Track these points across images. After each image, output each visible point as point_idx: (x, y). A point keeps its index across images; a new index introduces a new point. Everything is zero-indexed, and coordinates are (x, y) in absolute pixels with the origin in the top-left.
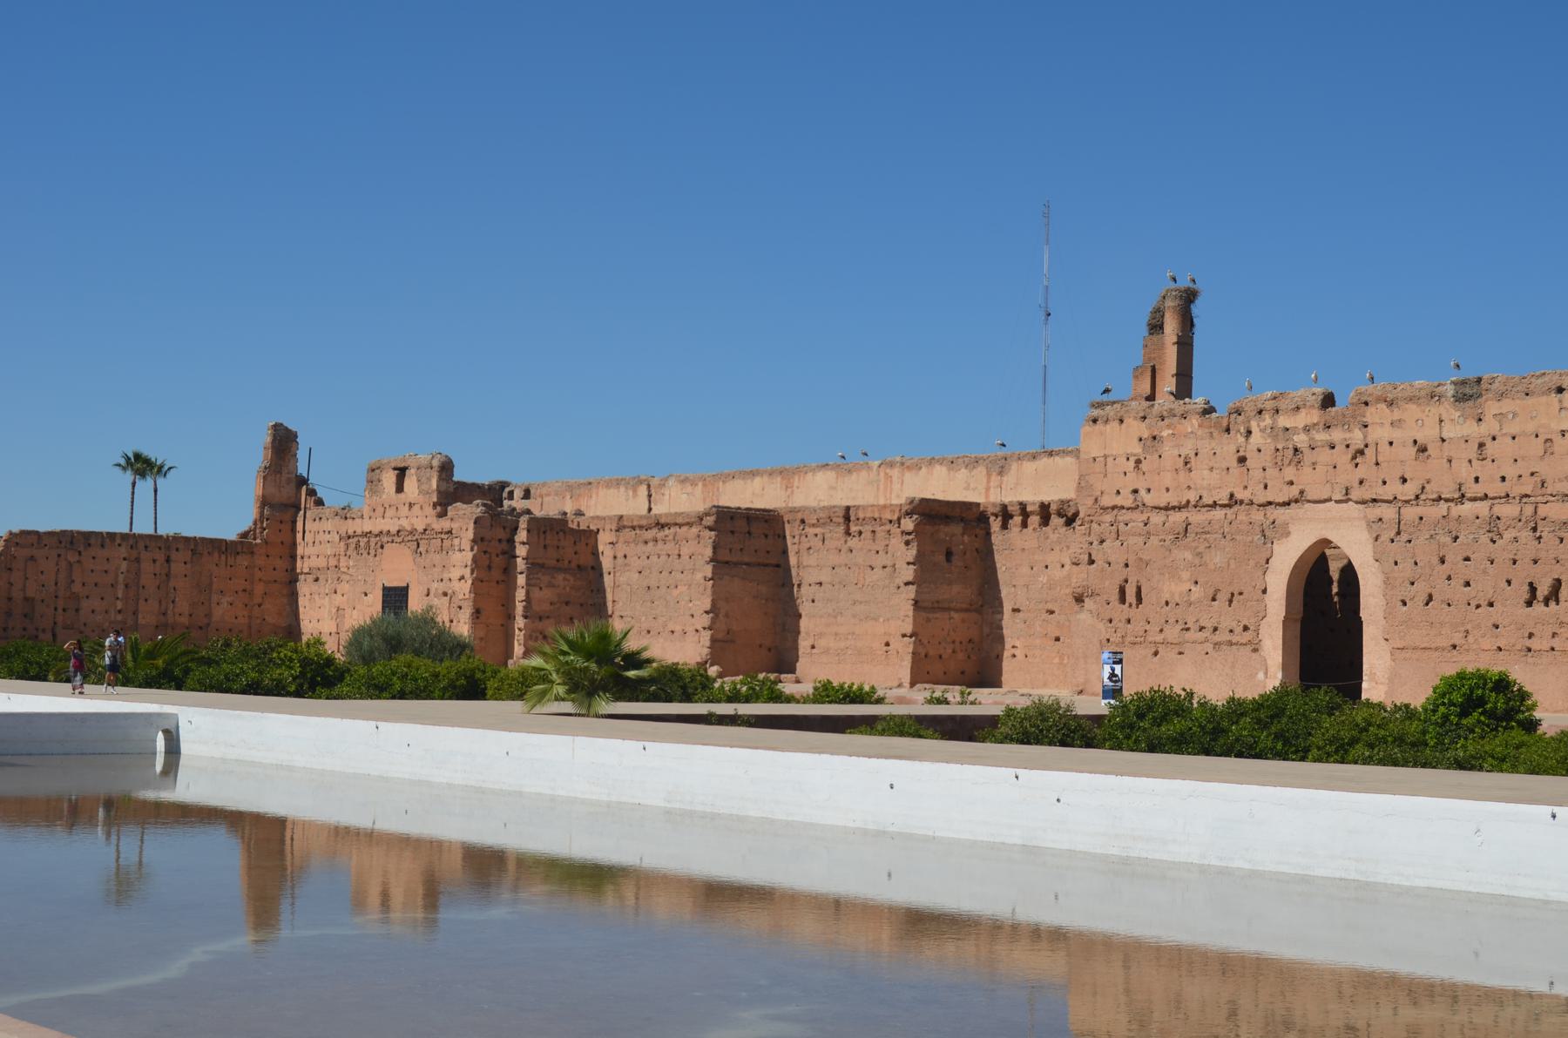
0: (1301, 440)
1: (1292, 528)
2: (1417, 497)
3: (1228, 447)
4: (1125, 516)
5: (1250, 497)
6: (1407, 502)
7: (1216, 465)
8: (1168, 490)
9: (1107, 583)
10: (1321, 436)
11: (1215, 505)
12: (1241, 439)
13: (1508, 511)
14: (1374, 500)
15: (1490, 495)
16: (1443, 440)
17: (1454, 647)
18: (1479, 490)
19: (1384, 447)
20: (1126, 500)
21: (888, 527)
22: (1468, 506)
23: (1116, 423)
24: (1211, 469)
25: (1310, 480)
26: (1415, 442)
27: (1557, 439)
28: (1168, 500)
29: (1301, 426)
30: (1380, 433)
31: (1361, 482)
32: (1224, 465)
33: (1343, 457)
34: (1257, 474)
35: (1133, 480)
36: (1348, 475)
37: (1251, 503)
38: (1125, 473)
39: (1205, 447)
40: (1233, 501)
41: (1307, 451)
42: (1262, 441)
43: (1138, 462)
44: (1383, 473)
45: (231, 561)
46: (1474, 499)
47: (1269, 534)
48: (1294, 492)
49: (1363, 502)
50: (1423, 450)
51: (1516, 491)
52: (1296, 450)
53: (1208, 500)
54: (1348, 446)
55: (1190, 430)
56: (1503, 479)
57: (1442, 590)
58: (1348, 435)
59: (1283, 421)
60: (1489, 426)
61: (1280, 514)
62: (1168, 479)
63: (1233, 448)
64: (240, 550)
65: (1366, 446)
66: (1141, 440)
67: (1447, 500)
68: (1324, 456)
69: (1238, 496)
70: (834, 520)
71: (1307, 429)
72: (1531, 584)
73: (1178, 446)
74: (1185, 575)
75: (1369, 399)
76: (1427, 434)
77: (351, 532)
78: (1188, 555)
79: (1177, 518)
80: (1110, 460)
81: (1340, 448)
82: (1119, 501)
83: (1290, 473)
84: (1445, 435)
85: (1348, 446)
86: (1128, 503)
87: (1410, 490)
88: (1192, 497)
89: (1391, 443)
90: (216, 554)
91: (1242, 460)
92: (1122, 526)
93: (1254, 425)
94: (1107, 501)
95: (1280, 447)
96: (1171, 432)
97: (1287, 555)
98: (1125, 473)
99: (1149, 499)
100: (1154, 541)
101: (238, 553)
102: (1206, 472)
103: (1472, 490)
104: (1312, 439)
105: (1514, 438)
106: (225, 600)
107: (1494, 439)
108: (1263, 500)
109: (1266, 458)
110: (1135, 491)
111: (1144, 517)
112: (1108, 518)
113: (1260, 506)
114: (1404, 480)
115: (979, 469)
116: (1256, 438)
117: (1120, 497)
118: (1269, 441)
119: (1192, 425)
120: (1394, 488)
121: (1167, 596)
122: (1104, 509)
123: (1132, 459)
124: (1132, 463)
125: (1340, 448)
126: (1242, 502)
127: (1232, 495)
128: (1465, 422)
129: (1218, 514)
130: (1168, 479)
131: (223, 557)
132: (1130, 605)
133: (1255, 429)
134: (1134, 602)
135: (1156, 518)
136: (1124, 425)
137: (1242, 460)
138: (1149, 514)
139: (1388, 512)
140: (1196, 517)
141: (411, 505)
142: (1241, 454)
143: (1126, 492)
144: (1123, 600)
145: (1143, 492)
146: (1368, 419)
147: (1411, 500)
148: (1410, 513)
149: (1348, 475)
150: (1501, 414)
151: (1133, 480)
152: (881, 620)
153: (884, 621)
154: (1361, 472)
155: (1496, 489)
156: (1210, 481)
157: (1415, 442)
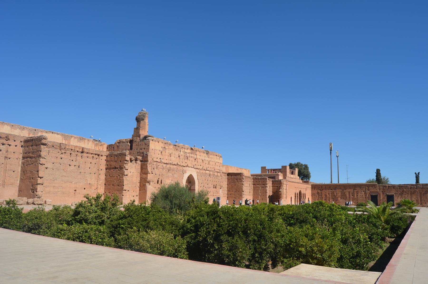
1: (187, 171)
2: (202, 169)
4: (158, 164)
5: (180, 164)
7: (175, 157)
8: (166, 160)
9: (155, 179)
10: (191, 155)
11: (175, 165)
12: (179, 152)
14: (197, 168)
19: (198, 159)
21: (77, 153)
22: (207, 172)
23: (157, 142)
24: (174, 157)
25: (189, 163)
28: (167, 162)
33: (194, 160)
34: (181, 160)
35: (160, 156)
38: (159, 154)
39: (174, 152)
40: (178, 164)
42: (182, 153)
46: (208, 170)
47: (184, 172)
48: (186, 164)
55: (171, 148)
58: (194, 156)
62: (167, 157)
63: (178, 154)
65: (196, 158)
66: (162, 147)
68: (191, 159)
69: (178, 164)
70: (54, 147)
72: (42, 177)
73: (169, 151)
74: (170, 179)
75: (197, 150)
76: (203, 158)
78: (171, 175)
80: (156, 150)
81: (193, 158)
82: (157, 160)
83: (186, 161)
84: (206, 159)
86: (159, 161)
88: (171, 162)
91: (179, 156)
93: (181, 150)
94: (155, 160)
95: (185, 155)
96: (168, 147)
98: (159, 154)
99: (163, 161)
100: (164, 170)
102: (173, 157)
104: (190, 155)
108: (182, 165)
112: (155, 163)
113: (181, 166)
115: (25, 131)
116: (182, 153)
117: (157, 159)
119: (172, 147)
120: (199, 167)
123: (160, 151)
124: (160, 153)
125: (193, 158)
129: (175, 166)
132: (160, 184)
133: (181, 151)
134: (160, 184)
135: (164, 165)
136: (159, 143)
139: (198, 171)
140: (172, 166)
142: (179, 155)
143: (159, 158)
144: (158, 182)
146: (197, 154)
148: (201, 171)
149: (194, 163)
151: (160, 156)
152: (73, 183)
153: (75, 183)
155: (210, 169)
156: (174, 160)
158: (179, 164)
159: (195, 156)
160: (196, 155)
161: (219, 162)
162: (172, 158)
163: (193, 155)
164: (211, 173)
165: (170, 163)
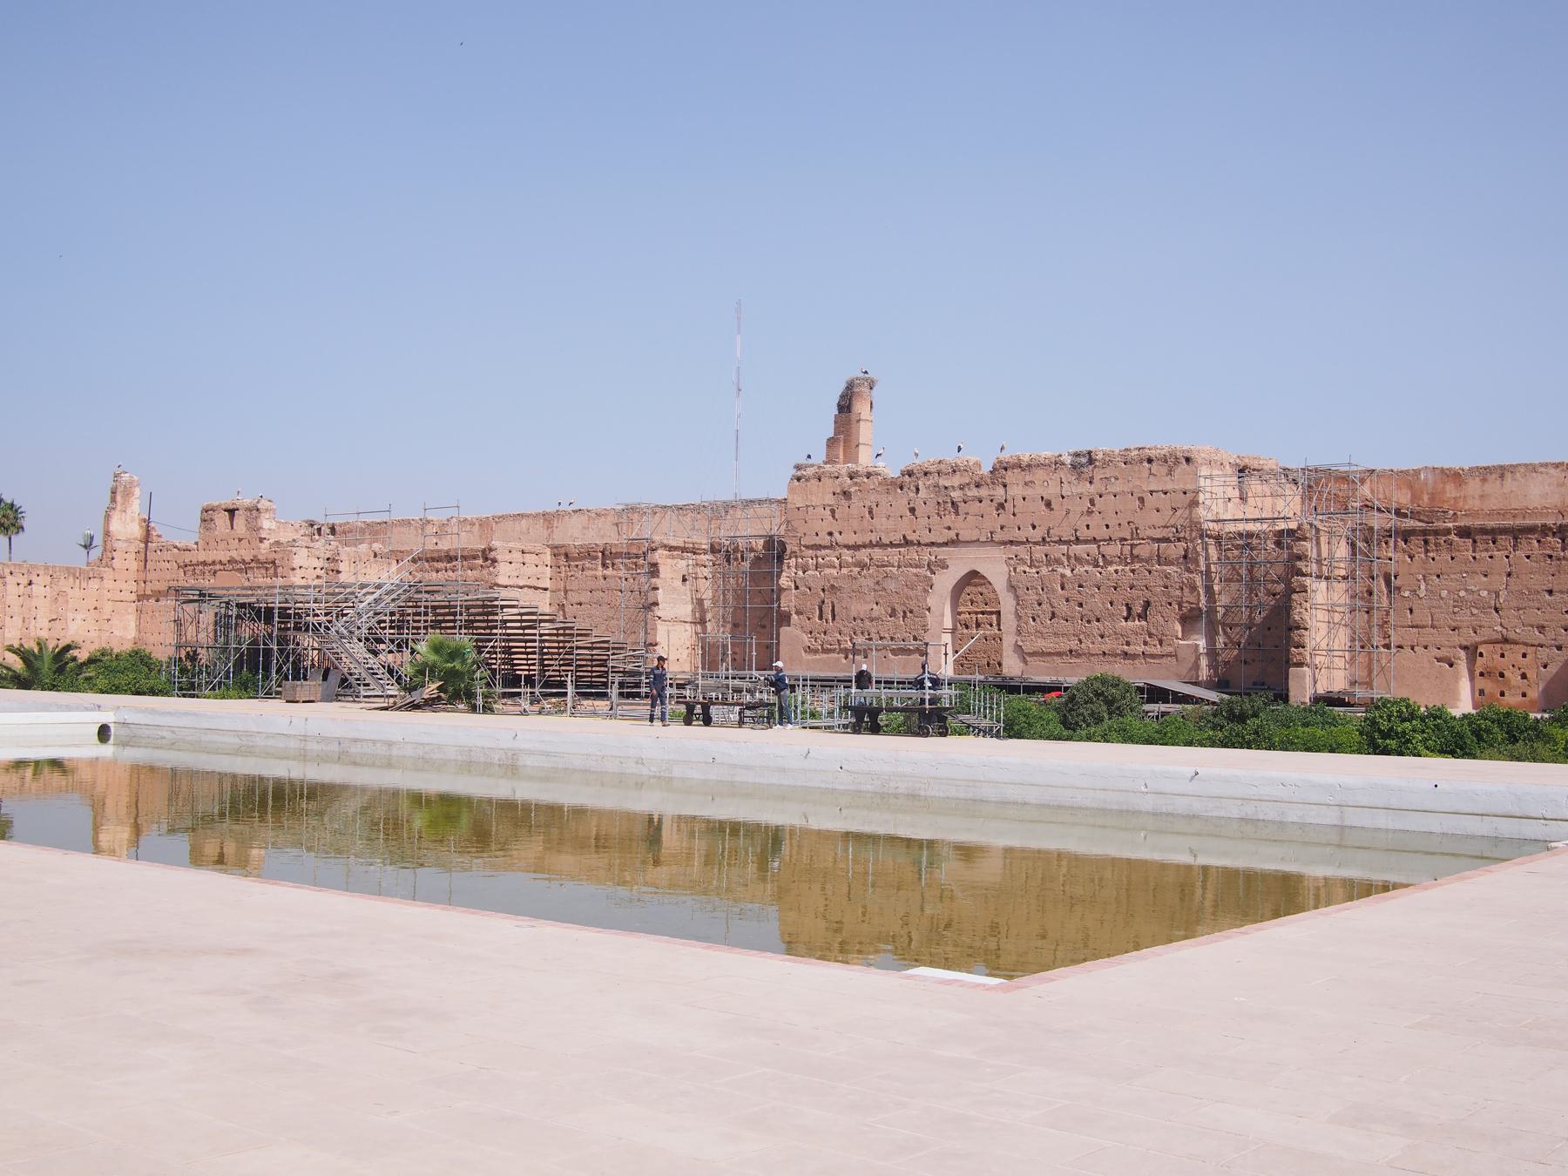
0: (956, 495)
3: (901, 501)
6: (1036, 543)
10: (973, 492)
11: (892, 545)
12: (912, 495)
13: (1112, 550)
15: (1098, 538)
16: (1063, 497)
17: (1071, 651)
18: (1088, 534)
20: (826, 540)
22: (1078, 549)
23: (814, 482)
26: (1042, 498)
27: (1148, 497)
29: (956, 485)
30: (1016, 491)
31: (1002, 528)
32: (898, 514)
36: (993, 520)
37: (919, 544)
40: (907, 543)
41: (962, 505)
43: (833, 512)
44: (1018, 521)
45: (84, 585)
46: (1086, 542)
48: (952, 534)
49: (1004, 543)
50: (1048, 504)
51: (1117, 534)
52: (953, 503)
53: (886, 541)
54: (992, 501)
56: (1107, 526)
57: (1063, 608)
59: (943, 482)
60: (1097, 487)
61: (943, 553)
62: (855, 524)
64: (91, 576)
65: (1006, 501)
66: (834, 494)
67: (1065, 543)
68: (974, 507)
71: (962, 488)
76: (1052, 491)
77: (187, 561)
79: (863, 555)
82: (817, 541)
83: (949, 519)
85: (992, 501)
87: (1037, 535)
88: (874, 538)
89: (1024, 499)
90: (71, 579)
92: (820, 559)
95: (940, 501)
97: (945, 581)
101: (513, 680)
103: (1084, 533)
105: (1115, 496)
106: (79, 617)
107: (1101, 496)
109: (931, 508)
110: (830, 534)
111: (837, 553)
114: (1034, 527)
116: (923, 494)
118: (932, 496)
121: (854, 614)
122: (807, 547)
123: (828, 508)
126: (912, 542)
127: (904, 537)
128: (1079, 483)
130: (855, 524)
131: (78, 581)
135: (847, 556)
137: (912, 510)
138: (840, 551)
139: (1022, 551)
140: (877, 553)
141: (240, 540)
142: (912, 505)
145: (836, 535)
146: (1007, 481)
147: (1039, 542)
150: (1106, 478)
154: (1002, 520)
155: (1104, 534)
157: (1042, 498)
158: (912, 537)
159: (1000, 491)
160: (1005, 486)
161: (1169, 487)
162: (881, 522)
163: (984, 492)
164: (1112, 550)
165: (871, 541)
